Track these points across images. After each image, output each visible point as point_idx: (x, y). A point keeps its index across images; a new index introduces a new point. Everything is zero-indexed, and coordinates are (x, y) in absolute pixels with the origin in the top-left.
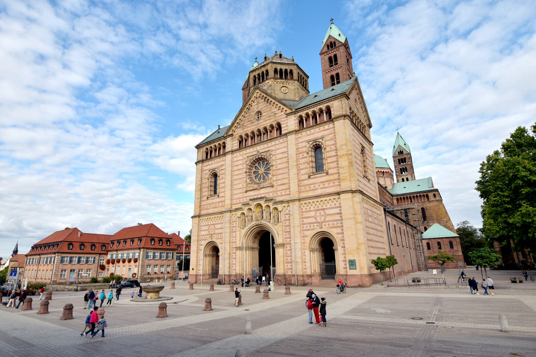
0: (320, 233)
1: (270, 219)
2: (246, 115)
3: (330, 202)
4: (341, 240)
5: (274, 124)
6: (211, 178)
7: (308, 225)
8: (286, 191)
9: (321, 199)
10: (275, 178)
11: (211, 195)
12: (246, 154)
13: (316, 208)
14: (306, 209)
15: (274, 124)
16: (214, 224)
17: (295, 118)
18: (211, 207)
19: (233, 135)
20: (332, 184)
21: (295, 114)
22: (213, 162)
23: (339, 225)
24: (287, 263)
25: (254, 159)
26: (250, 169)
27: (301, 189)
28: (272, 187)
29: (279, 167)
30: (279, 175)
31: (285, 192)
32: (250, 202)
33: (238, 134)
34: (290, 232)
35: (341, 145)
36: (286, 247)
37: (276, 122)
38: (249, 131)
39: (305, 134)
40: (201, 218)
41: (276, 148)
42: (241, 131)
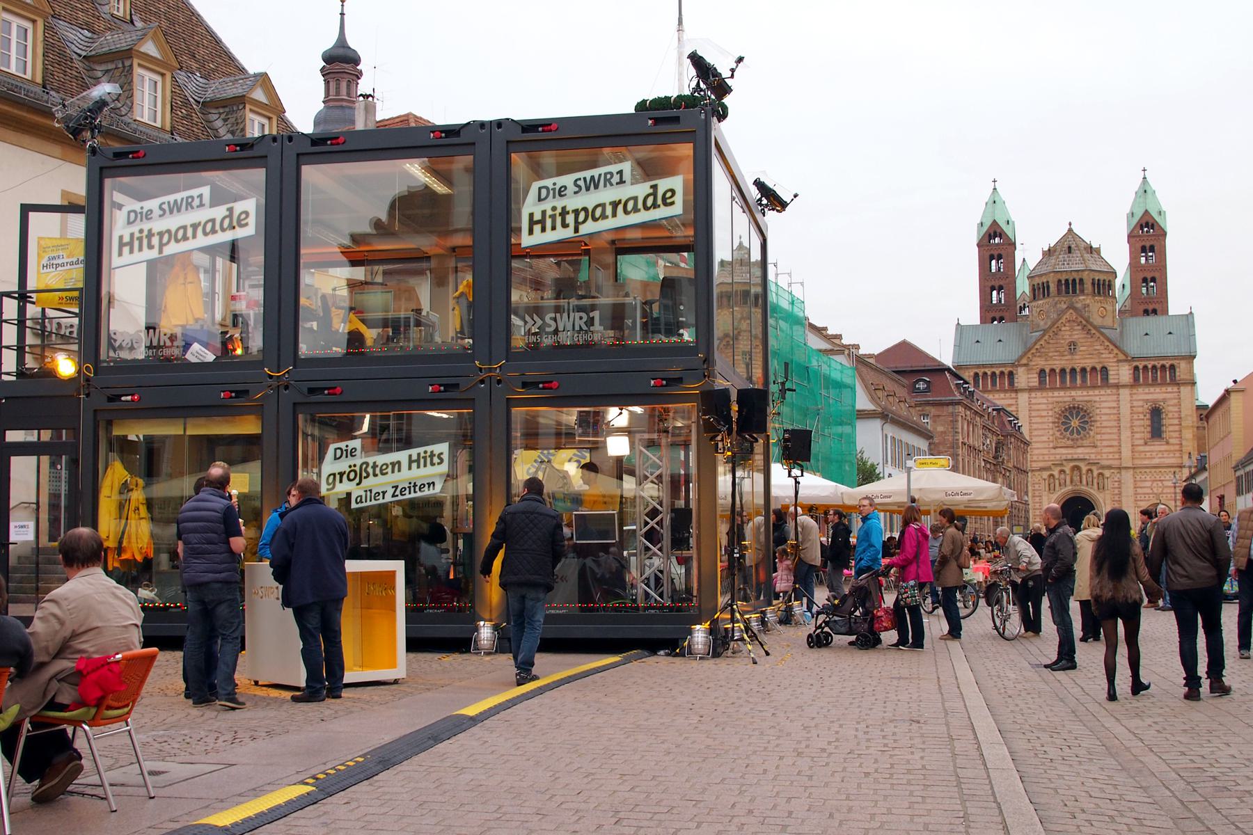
1: (1092, 485)
2: (1051, 341)
7: (1143, 496)
10: (1098, 437)
12: (1053, 397)
15: (1098, 368)
26: (1059, 419)
29: (1105, 424)
30: (1104, 434)
32: (1064, 463)
35: (1187, 415)
37: (1101, 365)
42: (1043, 363)
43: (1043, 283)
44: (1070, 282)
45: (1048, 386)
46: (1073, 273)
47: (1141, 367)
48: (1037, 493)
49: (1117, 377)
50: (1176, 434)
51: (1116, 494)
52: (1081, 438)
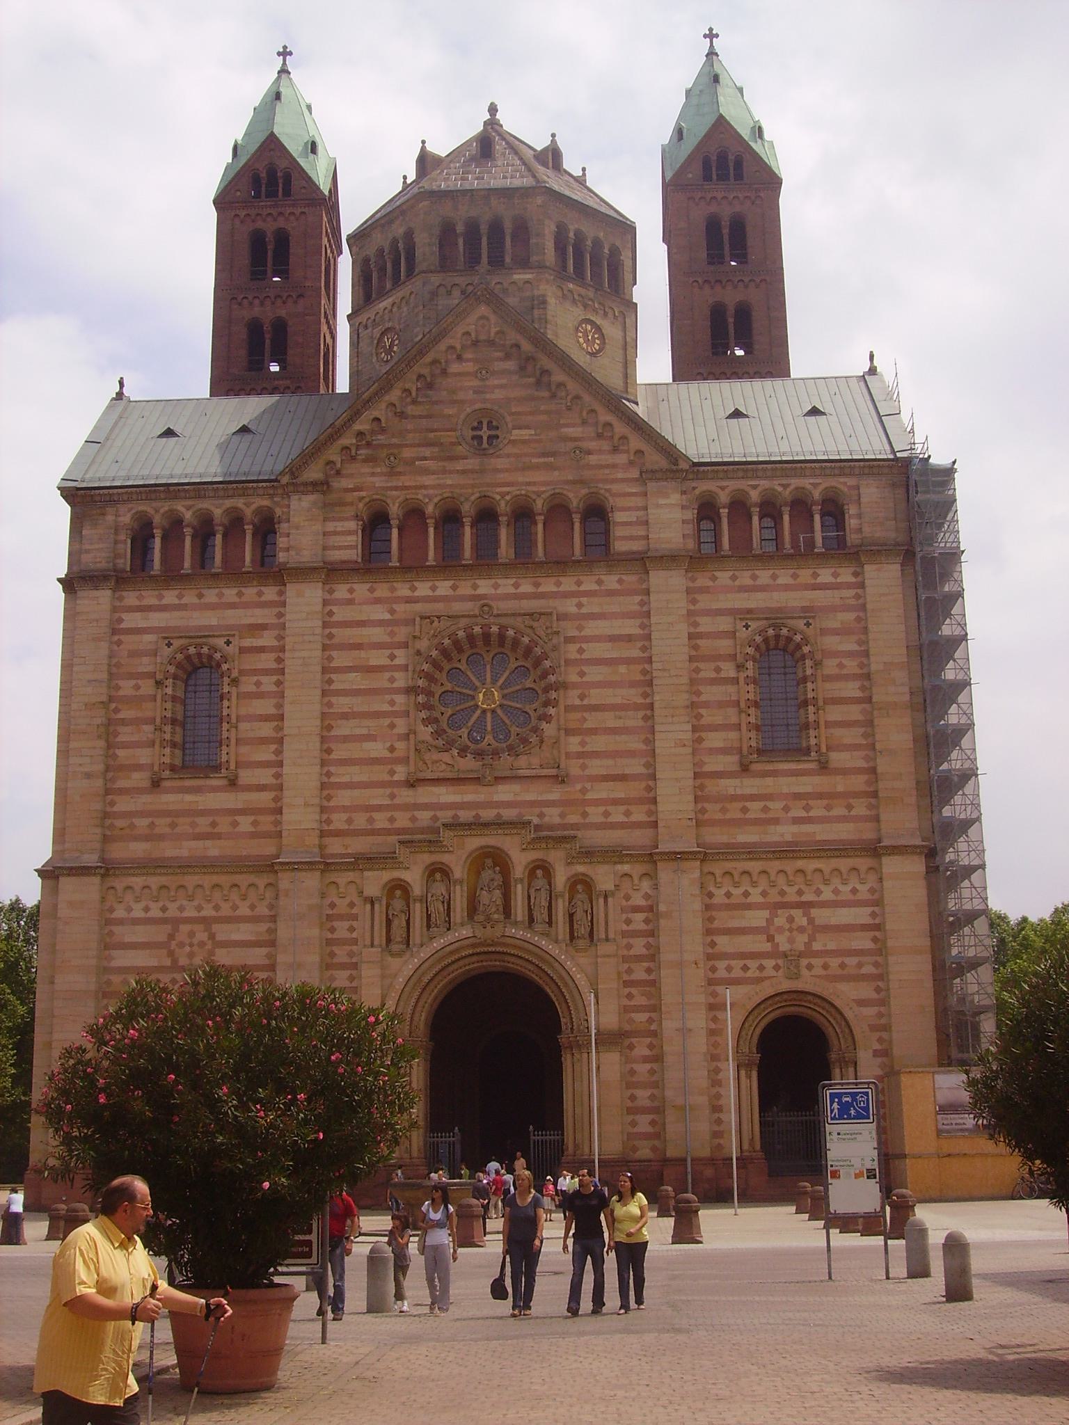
0: (785, 997)
1: (550, 923)
2: (410, 410)
3: (836, 882)
4: (873, 1028)
5: (575, 499)
6: (175, 677)
7: (737, 963)
8: (633, 808)
9: (800, 864)
10: (574, 743)
11: (173, 768)
12: (409, 600)
13: (774, 897)
14: (728, 895)
16: (206, 922)
17: (684, 496)
18: (177, 830)
19: (328, 487)
20: (839, 811)
21: (685, 479)
22: (190, 598)
23: (868, 969)
24: (630, 1111)
25: (461, 634)
26: (430, 678)
27: (703, 811)
28: (563, 781)
29: (596, 697)
30: (594, 731)
31: (627, 813)
32: (447, 836)
33: (357, 489)
34: (653, 983)
36: (631, 1047)
37: (584, 491)
38: (431, 492)
39: (729, 582)
40: (119, 884)
41: (584, 610)
42: (379, 482)
43: (395, 242)
44: (484, 229)
45: (395, 563)
46: (494, 201)
47: (724, 498)
48: (341, 954)
49: (641, 532)
50: (851, 736)
51: (639, 958)
52: (510, 748)
